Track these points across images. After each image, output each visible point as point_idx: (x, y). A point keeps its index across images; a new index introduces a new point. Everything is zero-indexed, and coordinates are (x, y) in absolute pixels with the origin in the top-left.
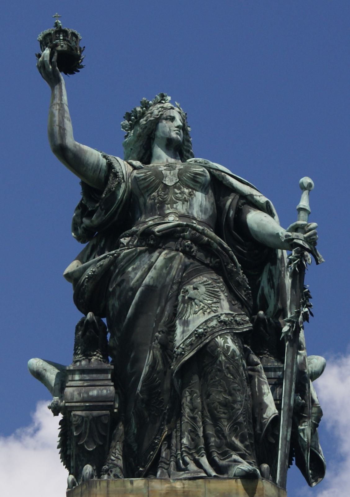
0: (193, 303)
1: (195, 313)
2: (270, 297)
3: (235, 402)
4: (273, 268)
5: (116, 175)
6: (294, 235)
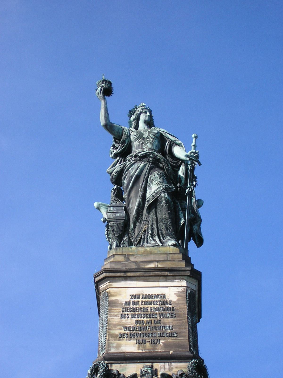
0: (153, 181)
1: (154, 185)
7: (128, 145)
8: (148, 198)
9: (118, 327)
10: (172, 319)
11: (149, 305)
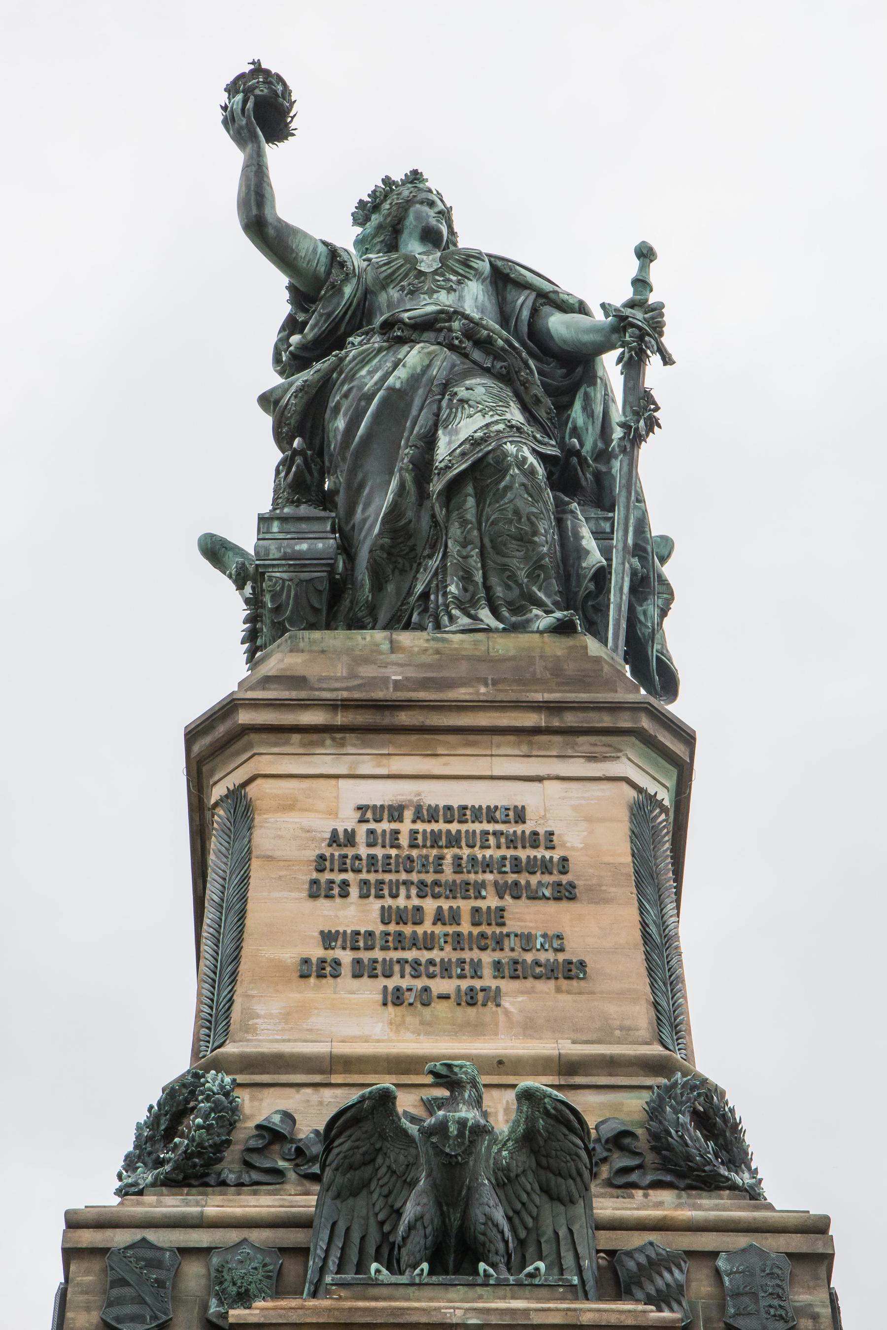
0: (466, 406)
1: (470, 416)
2: (587, 429)
3: (535, 533)
4: (590, 390)
5: (342, 265)
6: (628, 312)
7: (352, 308)
8: (441, 462)
11: (446, 851)
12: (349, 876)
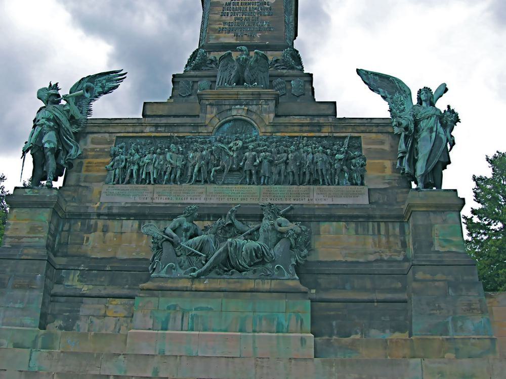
9: (219, 23)
10: (269, 16)
12: (229, 11)
